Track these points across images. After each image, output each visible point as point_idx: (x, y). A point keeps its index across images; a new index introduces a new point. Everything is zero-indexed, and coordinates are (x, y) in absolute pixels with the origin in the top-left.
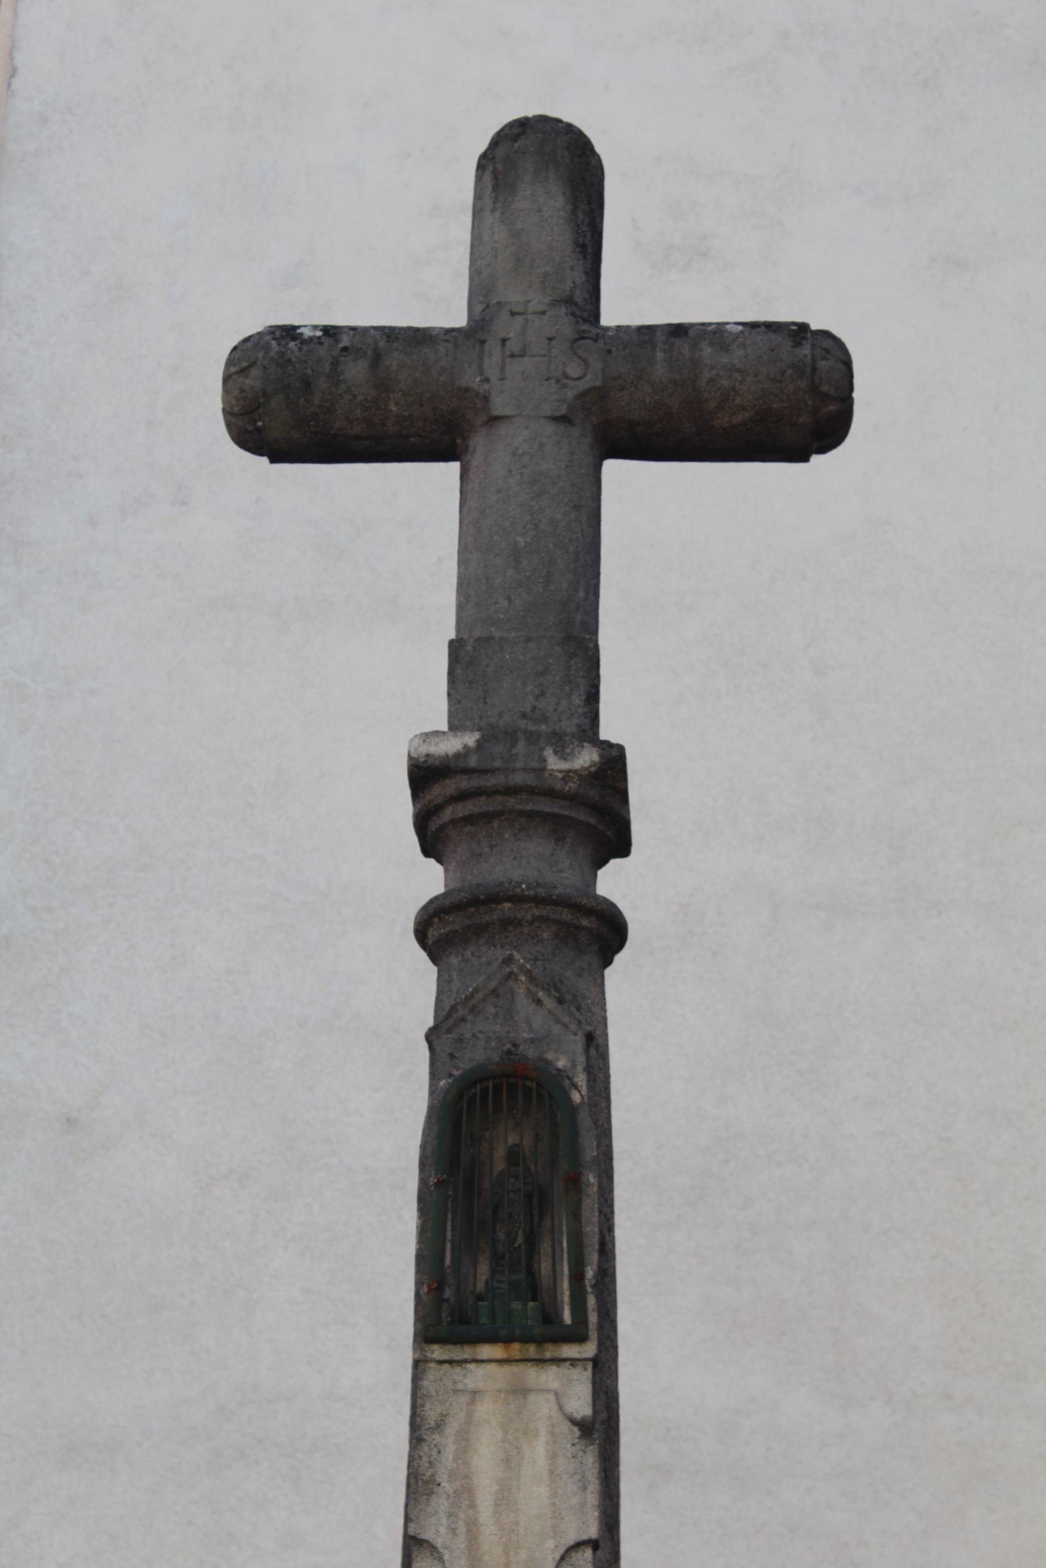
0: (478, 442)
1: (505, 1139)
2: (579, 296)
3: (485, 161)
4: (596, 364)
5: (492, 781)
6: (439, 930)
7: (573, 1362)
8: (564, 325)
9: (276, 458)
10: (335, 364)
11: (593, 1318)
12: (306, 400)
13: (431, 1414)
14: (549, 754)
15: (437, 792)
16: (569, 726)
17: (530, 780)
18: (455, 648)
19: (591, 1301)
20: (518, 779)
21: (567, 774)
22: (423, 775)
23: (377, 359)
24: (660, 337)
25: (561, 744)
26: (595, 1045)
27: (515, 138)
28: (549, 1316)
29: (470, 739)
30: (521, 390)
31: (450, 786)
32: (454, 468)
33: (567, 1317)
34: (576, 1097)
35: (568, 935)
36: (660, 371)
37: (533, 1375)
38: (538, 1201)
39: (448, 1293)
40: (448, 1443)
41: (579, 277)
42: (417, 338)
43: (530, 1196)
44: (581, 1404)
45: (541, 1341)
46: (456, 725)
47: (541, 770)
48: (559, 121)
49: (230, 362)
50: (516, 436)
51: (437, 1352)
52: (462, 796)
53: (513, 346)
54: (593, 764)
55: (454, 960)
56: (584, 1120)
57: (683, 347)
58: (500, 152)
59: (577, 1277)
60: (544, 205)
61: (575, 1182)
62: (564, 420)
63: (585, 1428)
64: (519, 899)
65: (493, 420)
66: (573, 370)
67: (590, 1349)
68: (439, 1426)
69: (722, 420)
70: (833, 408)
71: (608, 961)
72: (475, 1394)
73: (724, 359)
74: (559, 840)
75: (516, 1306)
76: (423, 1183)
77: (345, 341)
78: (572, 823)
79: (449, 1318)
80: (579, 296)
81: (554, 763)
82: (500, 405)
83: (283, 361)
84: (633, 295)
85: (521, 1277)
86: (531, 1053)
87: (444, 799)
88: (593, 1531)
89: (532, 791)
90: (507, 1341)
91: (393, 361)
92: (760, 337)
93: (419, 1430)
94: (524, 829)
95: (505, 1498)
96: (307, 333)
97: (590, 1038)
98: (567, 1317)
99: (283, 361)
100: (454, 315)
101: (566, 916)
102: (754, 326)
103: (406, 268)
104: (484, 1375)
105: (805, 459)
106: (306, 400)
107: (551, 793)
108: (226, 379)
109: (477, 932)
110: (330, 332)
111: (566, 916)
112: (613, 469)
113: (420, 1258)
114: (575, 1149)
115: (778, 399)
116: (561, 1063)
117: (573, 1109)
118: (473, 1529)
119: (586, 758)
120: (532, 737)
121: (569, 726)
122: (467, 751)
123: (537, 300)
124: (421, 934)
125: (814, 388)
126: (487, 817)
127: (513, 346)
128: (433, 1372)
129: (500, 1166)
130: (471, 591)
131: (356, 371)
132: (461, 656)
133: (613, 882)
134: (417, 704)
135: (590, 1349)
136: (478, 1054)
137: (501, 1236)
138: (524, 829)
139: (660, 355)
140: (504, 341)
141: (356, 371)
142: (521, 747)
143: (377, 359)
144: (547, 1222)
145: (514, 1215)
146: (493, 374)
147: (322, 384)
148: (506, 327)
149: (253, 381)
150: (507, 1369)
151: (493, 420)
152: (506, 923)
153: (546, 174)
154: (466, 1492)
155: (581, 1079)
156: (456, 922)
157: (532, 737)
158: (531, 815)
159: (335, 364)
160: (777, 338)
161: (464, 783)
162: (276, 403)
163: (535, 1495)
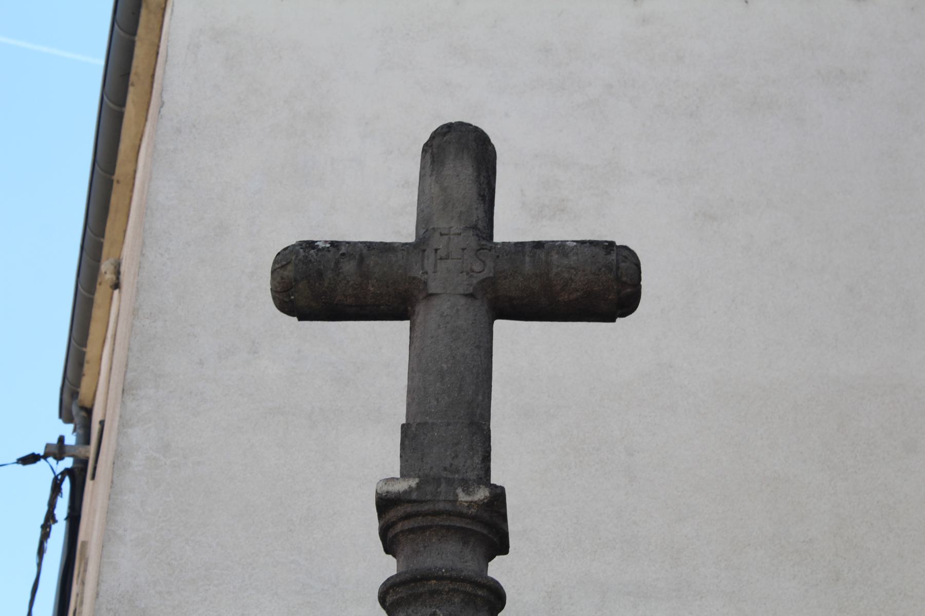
0: (420, 308)
2: (481, 225)
3: (427, 147)
4: (490, 264)
5: (426, 507)
8: (472, 241)
9: (303, 316)
10: (337, 263)
12: (322, 284)
14: (459, 491)
15: (392, 514)
16: (472, 475)
17: (448, 507)
20: (441, 506)
22: (385, 504)
24: (528, 249)
27: (445, 134)
29: (413, 482)
30: (446, 278)
31: (400, 511)
32: (406, 324)
35: (470, 600)
36: (528, 267)
41: (481, 214)
42: (386, 248)
46: (404, 474)
47: (456, 501)
48: (470, 125)
52: (408, 517)
54: (486, 497)
58: (436, 142)
60: (460, 174)
62: (471, 296)
65: (430, 296)
66: (477, 267)
69: (564, 297)
70: (629, 290)
73: (565, 262)
74: (465, 543)
77: (343, 250)
80: (481, 225)
81: (463, 497)
82: (433, 287)
83: (307, 261)
84: (511, 225)
87: (397, 518)
89: (449, 514)
91: (371, 261)
96: (321, 245)
99: (307, 261)
101: (469, 588)
102: (583, 242)
103: (381, 207)
105: (613, 320)
106: (322, 284)
107: (461, 515)
108: (273, 272)
109: (415, 598)
111: (469, 588)
112: (500, 326)
115: (598, 285)
119: (482, 494)
120: (450, 482)
121: (472, 475)
123: (456, 227)
124: (382, 599)
125: (618, 279)
126: (423, 529)
127: (442, 253)
130: (416, 395)
131: (349, 267)
133: (497, 569)
139: (527, 259)
140: (436, 250)
141: (349, 267)
142: (443, 486)
143: (362, 260)
147: (329, 275)
148: (439, 242)
149: (289, 272)
151: (430, 296)
152: (433, 593)
153: (462, 156)
156: (403, 592)
157: (450, 482)
158: (448, 528)
159: (337, 263)
160: (596, 250)
161: (409, 509)
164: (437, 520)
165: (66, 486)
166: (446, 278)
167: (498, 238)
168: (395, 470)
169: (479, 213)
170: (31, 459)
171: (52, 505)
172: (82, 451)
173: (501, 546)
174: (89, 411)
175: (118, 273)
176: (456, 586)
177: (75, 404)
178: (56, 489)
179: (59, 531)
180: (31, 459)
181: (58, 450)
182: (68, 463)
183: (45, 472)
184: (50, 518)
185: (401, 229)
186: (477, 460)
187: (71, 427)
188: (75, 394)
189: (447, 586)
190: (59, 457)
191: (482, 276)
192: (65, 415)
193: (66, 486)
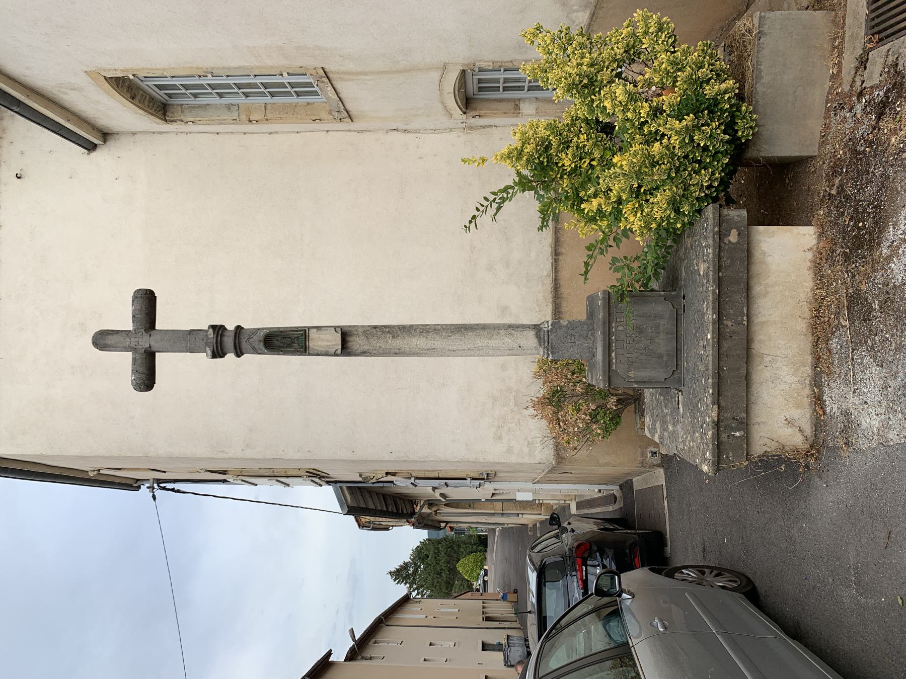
0: (153, 349)
6: (239, 354)
12: (146, 378)
42: (134, 360)
44: (315, 330)
50: (153, 344)
60: (111, 340)
84: (129, 326)
87: (218, 353)
93: (318, 355)
94: (222, 342)
95: (327, 341)
103: (122, 363)
106: (146, 378)
112: (157, 327)
115: (147, 302)
119: (211, 330)
124: (239, 356)
133: (231, 327)
134: (202, 359)
136: (261, 346)
138: (222, 342)
145: (284, 341)
148: (133, 344)
153: (103, 340)
163: (329, 337)
165: (162, 485)
166: (145, 342)
170: (154, 497)
173: (222, 327)
178: (164, 488)
179: (177, 486)
180: (154, 497)
181: (151, 488)
182: (155, 485)
183: (158, 493)
184: (173, 490)
185: (129, 355)
192: (138, 488)
193: (162, 485)
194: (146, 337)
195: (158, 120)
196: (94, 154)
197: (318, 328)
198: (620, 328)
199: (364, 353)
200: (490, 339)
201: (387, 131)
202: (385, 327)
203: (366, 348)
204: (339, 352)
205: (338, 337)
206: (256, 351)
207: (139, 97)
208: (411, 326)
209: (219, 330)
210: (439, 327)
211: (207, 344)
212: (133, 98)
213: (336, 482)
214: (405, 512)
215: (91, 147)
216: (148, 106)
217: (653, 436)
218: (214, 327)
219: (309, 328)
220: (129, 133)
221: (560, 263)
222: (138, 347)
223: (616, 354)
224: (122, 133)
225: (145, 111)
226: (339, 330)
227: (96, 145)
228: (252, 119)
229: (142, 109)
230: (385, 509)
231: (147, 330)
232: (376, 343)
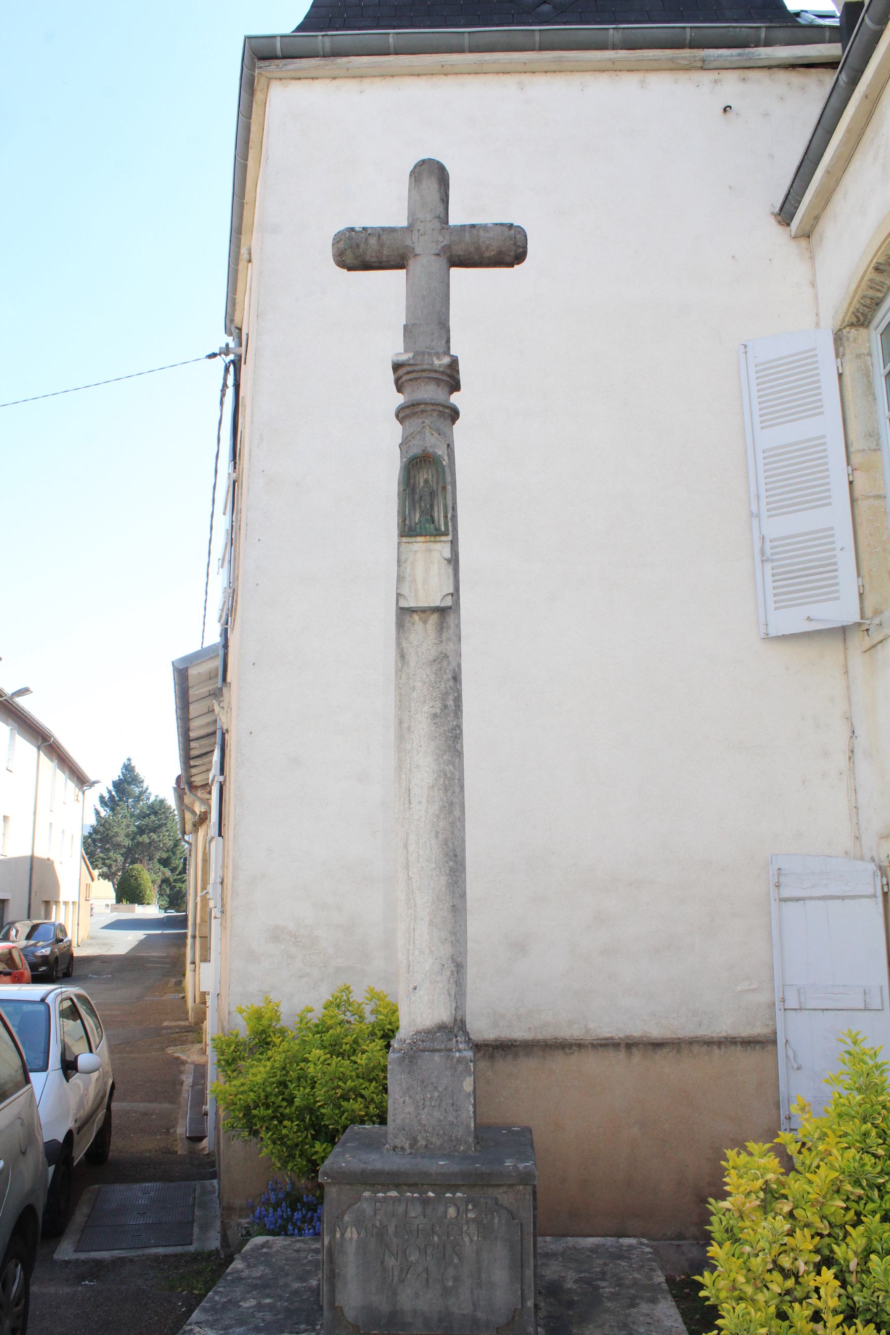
0: (411, 263)
1: (423, 476)
2: (442, 216)
3: (412, 173)
4: (447, 237)
5: (417, 368)
6: (404, 414)
7: (445, 542)
8: (437, 225)
9: (350, 268)
10: (366, 239)
11: (450, 529)
13: (403, 558)
17: (429, 367)
18: (406, 327)
19: (450, 524)
20: (425, 367)
21: (440, 366)
22: (396, 367)
23: (379, 237)
24: (467, 228)
25: (437, 355)
26: (450, 447)
28: (437, 529)
29: (411, 355)
32: (404, 271)
33: (443, 529)
34: (444, 463)
35: (441, 414)
36: (467, 238)
37: (432, 546)
38: (432, 494)
39: (407, 522)
40: (408, 566)
42: (392, 230)
43: (431, 493)
44: (447, 554)
45: (435, 536)
49: (334, 239)
51: (404, 539)
52: (408, 373)
53: (422, 232)
55: (407, 423)
56: (447, 470)
57: (475, 231)
58: (417, 170)
59: (446, 517)
60: (431, 186)
61: (444, 488)
62: (438, 255)
63: (449, 561)
64: (427, 404)
66: (441, 239)
67: (450, 538)
68: (405, 561)
69: (487, 254)
70: (521, 250)
71: (453, 423)
72: (416, 552)
73: (487, 235)
74: (438, 386)
75: (428, 526)
76: (399, 489)
77: (369, 232)
78: (443, 380)
79: (408, 531)
81: (437, 362)
82: (418, 250)
83: (350, 238)
85: (428, 517)
86: (431, 450)
87: (403, 374)
88: (451, 591)
89: (430, 371)
90: (426, 536)
92: (498, 227)
94: (428, 383)
96: (358, 229)
97: (448, 445)
98: (443, 529)
99: (350, 238)
100: (403, 222)
101: (441, 409)
102: (497, 224)
103: (386, 206)
104: (419, 545)
107: (436, 371)
108: (333, 245)
109: (414, 414)
110: (364, 229)
111: (441, 409)
112: (453, 271)
113: (398, 512)
114: (444, 478)
116: (440, 453)
117: (443, 467)
118: (416, 590)
119: (446, 360)
120: (429, 354)
121: (441, 350)
122: (410, 359)
123: (429, 217)
124: (397, 416)
125: (515, 244)
126: (416, 379)
127: (422, 232)
128: (403, 546)
129: (422, 484)
132: (408, 330)
133: (455, 399)
135: (450, 538)
136: (415, 451)
137: (423, 505)
138: (428, 383)
141: (373, 241)
142: (426, 357)
143: (379, 237)
144: (436, 501)
146: (415, 240)
147: (362, 246)
148: (419, 226)
149: (341, 245)
150: (425, 544)
152: (422, 411)
154: (414, 580)
155: (446, 458)
156: (407, 411)
158: (429, 378)
159: (366, 239)
160: (503, 228)
161: (409, 369)
162: (348, 252)
164: (424, 374)
167: (452, 222)
168: (400, 348)
169: (440, 209)
170: (213, 355)
171: (225, 379)
172: (238, 351)
173: (455, 386)
174: (240, 329)
175: (250, 254)
176: (435, 407)
177: (233, 327)
178: (227, 370)
179: (230, 392)
180: (213, 355)
181: (226, 351)
184: (225, 385)
186: (443, 342)
187: (232, 338)
188: (232, 321)
189: (429, 408)
190: (227, 354)
191: (443, 244)
192: (228, 332)
194: (435, 249)
195: (841, 315)
196: (772, 221)
197: (454, 561)
198: (452, 1212)
199: (402, 655)
200: (431, 923)
201: (849, 719)
202: (458, 700)
203: (412, 659)
204: (404, 604)
205: (436, 601)
206: (404, 445)
207: (878, 278)
208: (459, 754)
209: (451, 379)
210: (457, 813)
211: (416, 354)
212: (877, 269)
213: (226, 646)
214: (194, 771)
215: (785, 214)
216: (864, 297)
217: (244, 1259)
218: (454, 364)
219: (454, 544)
220: (814, 275)
221: (611, 1054)
222: (415, 238)
223: (395, 1199)
224: (813, 266)
225: (856, 291)
226: (448, 602)
227: (788, 225)
228: (857, 473)
229: (859, 286)
230: (192, 735)
231: (447, 249)
232: (421, 676)
